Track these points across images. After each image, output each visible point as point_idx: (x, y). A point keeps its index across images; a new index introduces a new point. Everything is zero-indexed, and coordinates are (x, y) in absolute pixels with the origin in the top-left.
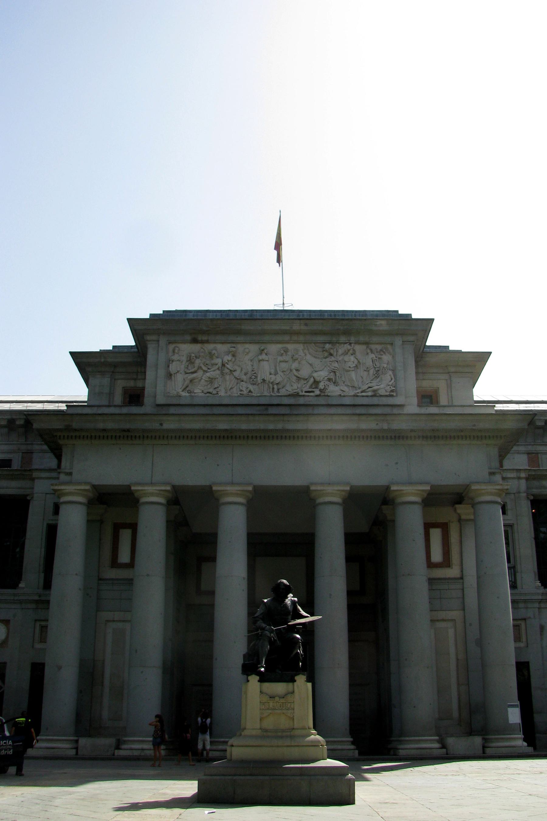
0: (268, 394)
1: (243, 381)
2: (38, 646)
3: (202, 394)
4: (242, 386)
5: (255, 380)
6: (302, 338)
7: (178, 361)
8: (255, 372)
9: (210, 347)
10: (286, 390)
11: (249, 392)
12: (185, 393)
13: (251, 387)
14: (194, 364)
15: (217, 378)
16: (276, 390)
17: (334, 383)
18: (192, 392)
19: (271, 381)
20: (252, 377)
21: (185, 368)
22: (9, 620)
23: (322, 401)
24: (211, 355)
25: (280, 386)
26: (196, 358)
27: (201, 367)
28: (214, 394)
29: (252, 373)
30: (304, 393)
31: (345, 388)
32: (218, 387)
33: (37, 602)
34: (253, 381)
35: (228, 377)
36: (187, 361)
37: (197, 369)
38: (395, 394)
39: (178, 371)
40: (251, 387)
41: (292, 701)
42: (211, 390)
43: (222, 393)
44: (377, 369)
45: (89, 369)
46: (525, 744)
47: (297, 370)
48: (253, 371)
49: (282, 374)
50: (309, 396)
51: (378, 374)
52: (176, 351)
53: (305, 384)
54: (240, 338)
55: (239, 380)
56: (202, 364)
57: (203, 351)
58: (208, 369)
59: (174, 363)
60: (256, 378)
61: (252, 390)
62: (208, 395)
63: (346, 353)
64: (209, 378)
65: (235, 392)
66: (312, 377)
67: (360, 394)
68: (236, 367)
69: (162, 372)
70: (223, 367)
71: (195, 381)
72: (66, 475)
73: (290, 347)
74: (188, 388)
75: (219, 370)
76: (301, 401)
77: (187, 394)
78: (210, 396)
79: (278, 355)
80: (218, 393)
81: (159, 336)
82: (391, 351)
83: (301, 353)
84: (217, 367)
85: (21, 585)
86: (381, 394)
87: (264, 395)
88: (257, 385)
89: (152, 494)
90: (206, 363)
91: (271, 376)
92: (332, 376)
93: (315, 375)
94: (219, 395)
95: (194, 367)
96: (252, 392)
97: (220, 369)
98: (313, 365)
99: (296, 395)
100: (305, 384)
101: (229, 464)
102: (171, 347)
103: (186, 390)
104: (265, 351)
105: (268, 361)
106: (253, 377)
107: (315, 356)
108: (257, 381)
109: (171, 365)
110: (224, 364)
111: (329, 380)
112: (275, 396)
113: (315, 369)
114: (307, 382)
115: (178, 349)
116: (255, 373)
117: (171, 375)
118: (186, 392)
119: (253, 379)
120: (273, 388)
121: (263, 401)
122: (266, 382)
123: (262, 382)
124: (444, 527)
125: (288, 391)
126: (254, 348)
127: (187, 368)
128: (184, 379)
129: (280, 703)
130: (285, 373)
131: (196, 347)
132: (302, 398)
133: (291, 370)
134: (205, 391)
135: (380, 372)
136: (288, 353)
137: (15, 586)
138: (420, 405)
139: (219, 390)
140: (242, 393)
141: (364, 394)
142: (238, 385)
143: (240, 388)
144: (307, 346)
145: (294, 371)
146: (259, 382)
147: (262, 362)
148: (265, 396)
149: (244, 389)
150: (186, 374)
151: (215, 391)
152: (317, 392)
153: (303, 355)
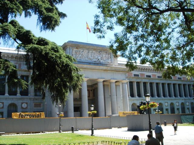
2: (34, 108)
6: (96, 50)
33: (34, 99)
40: (88, 59)
51: (108, 59)
54: (85, 49)
55: (85, 57)
63: (103, 54)
73: (94, 51)
76: (96, 63)
85: (29, 95)
99: (95, 61)
121: (90, 62)
126: (87, 51)
131: (77, 49)
152: (99, 61)
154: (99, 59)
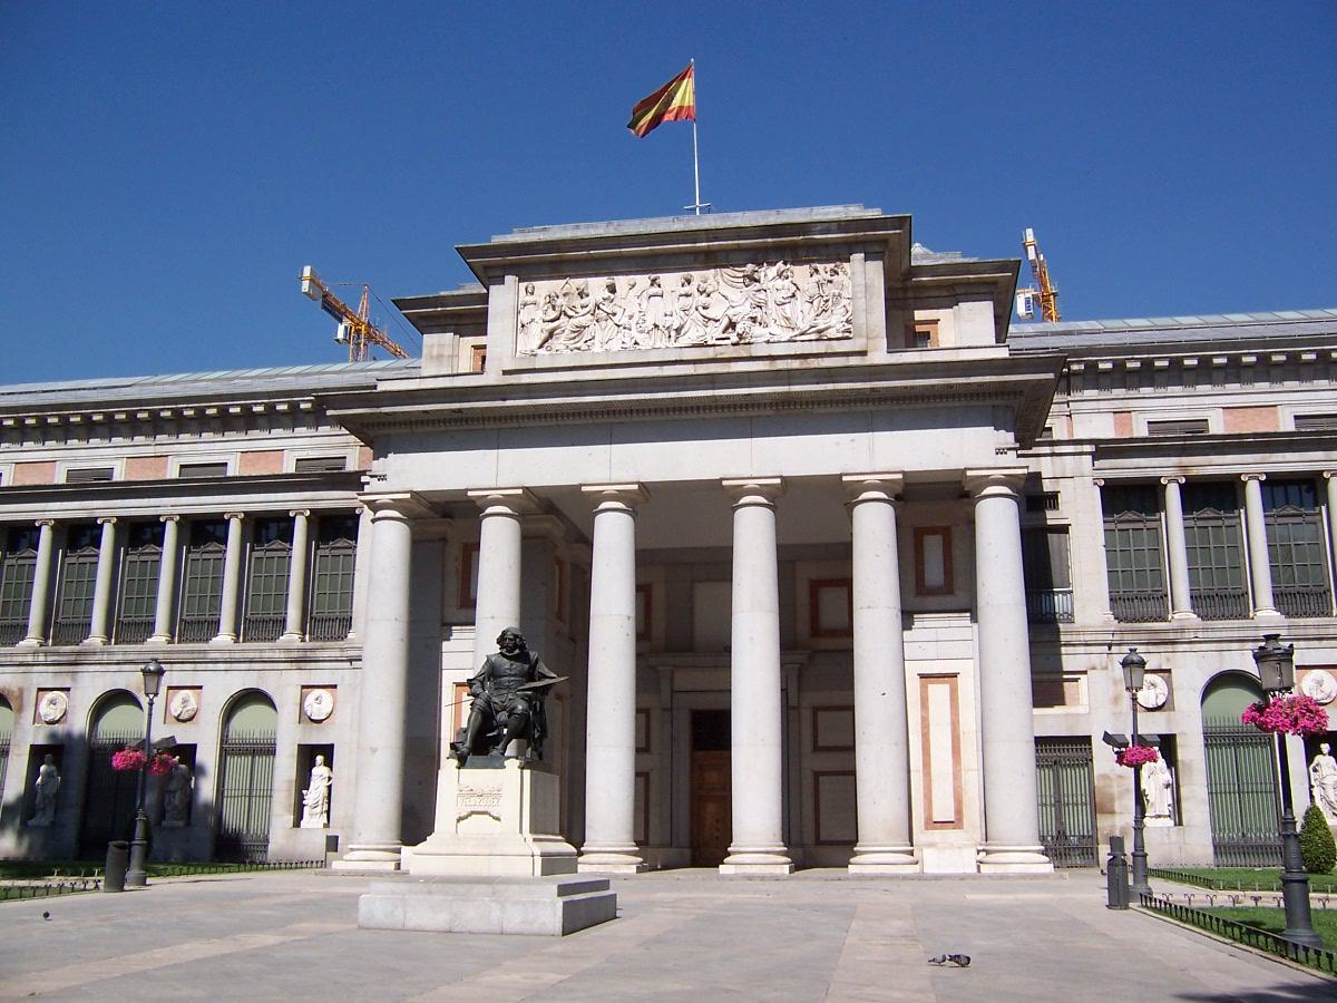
9: (576, 283)
16: (673, 338)
17: (760, 324)
22: (335, 687)
23: (742, 352)
31: (773, 328)
35: (603, 323)
38: (851, 336)
39: (533, 320)
40: (639, 338)
42: (578, 345)
43: (597, 348)
44: (825, 298)
46: (1047, 859)
52: (530, 290)
63: (780, 275)
65: (615, 346)
67: (798, 338)
68: (616, 310)
69: (509, 322)
76: (710, 353)
77: (547, 353)
82: (848, 271)
84: (588, 309)
85: (349, 636)
86: (829, 336)
89: (496, 502)
91: (668, 318)
92: (757, 313)
99: (704, 345)
111: (754, 319)
113: (733, 304)
124: (946, 533)
126: (643, 280)
135: (830, 303)
137: (343, 637)
138: (891, 349)
141: (803, 338)
145: (700, 309)
149: (627, 340)
152: (734, 338)
154: (732, 325)
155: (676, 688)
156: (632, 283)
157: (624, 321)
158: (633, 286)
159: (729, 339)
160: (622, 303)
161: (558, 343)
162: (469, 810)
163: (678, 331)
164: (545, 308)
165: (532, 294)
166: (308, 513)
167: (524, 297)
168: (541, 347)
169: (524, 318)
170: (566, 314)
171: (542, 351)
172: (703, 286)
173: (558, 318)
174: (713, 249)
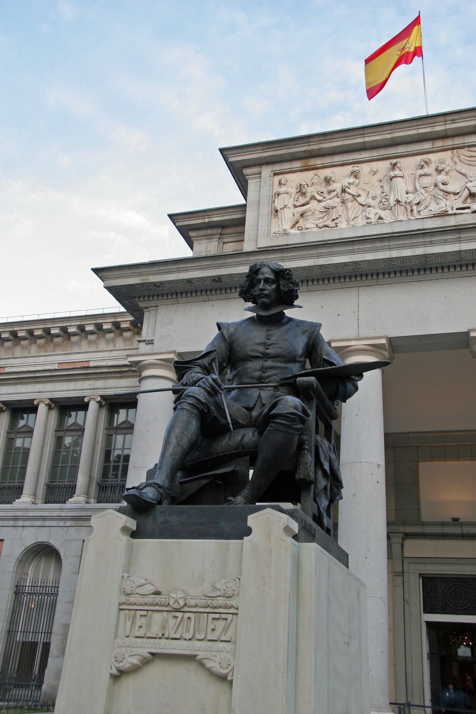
0: (406, 219)
1: (369, 207)
3: (316, 230)
4: (369, 214)
5: (386, 203)
6: (449, 143)
7: (285, 193)
8: (385, 194)
10: (430, 210)
11: (378, 219)
12: (295, 230)
13: (383, 214)
14: (305, 195)
15: (336, 207)
16: (415, 212)
18: (304, 228)
19: (408, 201)
20: (382, 201)
21: (295, 201)
24: (328, 181)
25: (422, 208)
26: (308, 187)
27: (314, 196)
28: (331, 227)
29: (382, 195)
30: (455, 211)
32: (337, 218)
34: (384, 205)
35: (349, 204)
36: (297, 193)
37: (309, 200)
39: (286, 206)
40: (383, 214)
41: (232, 611)
42: (329, 223)
43: (343, 225)
45: (192, 234)
47: (443, 184)
48: (383, 192)
49: (422, 191)
50: (462, 214)
52: (283, 182)
53: (455, 199)
56: (316, 193)
57: (318, 178)
58: (324, 198)
59: (281, 196)
60: (388, 200)
61: (383, 216)
62: (323, 229)
64: (325, 208)
65: (361, 222)
66: (466, 190)
68: (360, 192)
69: (265, 209)
70: (343, 195)
71: (307, 214)
72: (147, 344)
74: (298, 224)
75: (338, 197)
76: (451, 222)
78: (328, 230)
79: (417, 169)
80: (338, 225)
81: (261, 167)
83: (449, 162)
87: (398, 220)
88: (390, 209)
90: (320, 191)
93: (469, 185)
94: (339, 227)
95: (306, 198)
96: (382, 219)
97: (339, 196)
98: (467, 175)
99: (444, 214)
100: (455, 199)
101: (354, 312)
102: (277, 179)
103: (295, 227)
104: (398, 165)
105: (403, 177)
106: (384, 200)
107: (469, 163)
108: (389, 204)
109: (276, 200)
110: (345, 190)
112: (414, 219)
113: (469, 179)
114: (459, 197)
115: (285, 179)
116: (387, 195)
117: (277, 211)
118: (296, 229)
119: (384, 202)
120: (412, 211)
122: (401, 204)
123: (395, 204)
125: (432, 211)
127: (297, 201)
128: (294, 215)
129: (187, 615)
130: (427, 190)
132: (453, 217)
133: (436, 186)
134: (321, 225)
136: (431, 165)
139: (338, 222)
140: (369, 221)
142: (364, 212)
143: (366, 216)
144: (457, 152)
146: (392, 204)
147: (394, 180)
148: (401, 221)
149: (372, 216)
150: (296, 208)
151: (334, 223)
153: (452, 164)
155: (405, 556)
156: (375, 169)
157: (370, 201)
158: (375, 173)
159: (469, 208)
160: (366, 187)
161: (310, 223)
162: (145, 652)
163: (418, 204)
164: (297, 196)
165: (284, 184)
166: (99, 399)
167: (276, 189)
168: (293, 227)
169: (278, 204)
170: (313, 198)
171: (293, 231)
172: (441, 167)
173: (307, 203)
174: (449, 133)
